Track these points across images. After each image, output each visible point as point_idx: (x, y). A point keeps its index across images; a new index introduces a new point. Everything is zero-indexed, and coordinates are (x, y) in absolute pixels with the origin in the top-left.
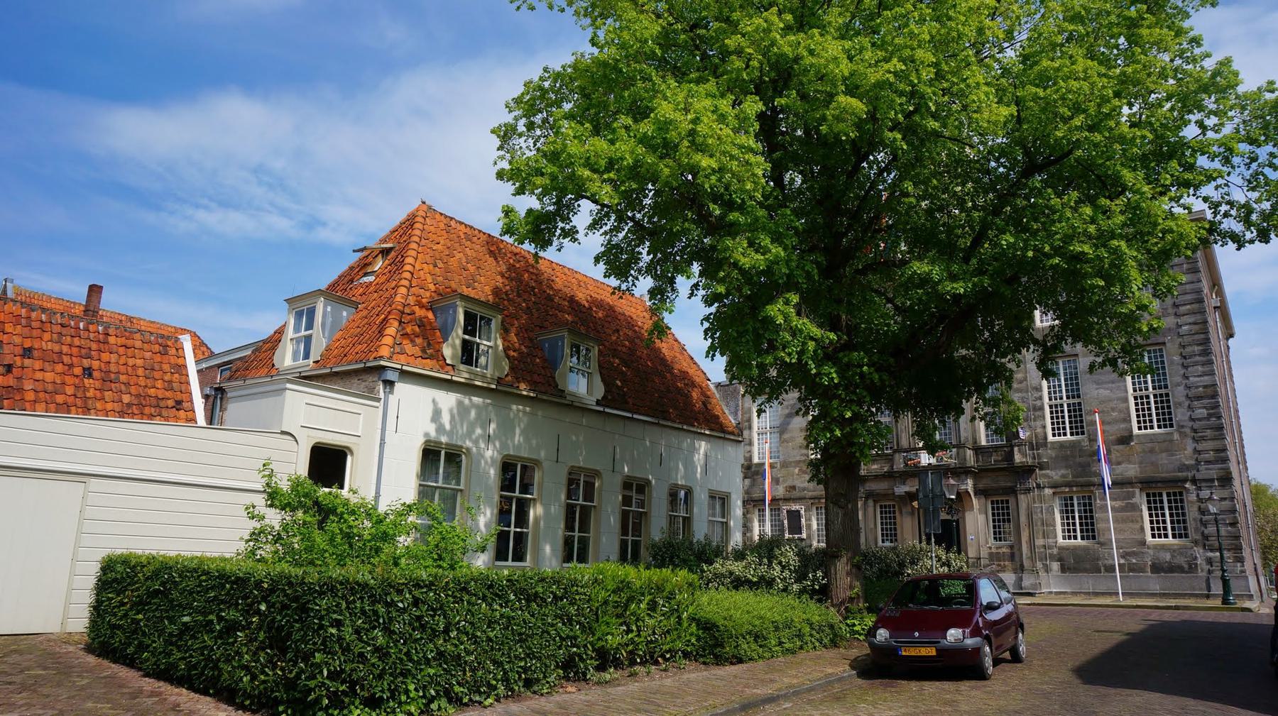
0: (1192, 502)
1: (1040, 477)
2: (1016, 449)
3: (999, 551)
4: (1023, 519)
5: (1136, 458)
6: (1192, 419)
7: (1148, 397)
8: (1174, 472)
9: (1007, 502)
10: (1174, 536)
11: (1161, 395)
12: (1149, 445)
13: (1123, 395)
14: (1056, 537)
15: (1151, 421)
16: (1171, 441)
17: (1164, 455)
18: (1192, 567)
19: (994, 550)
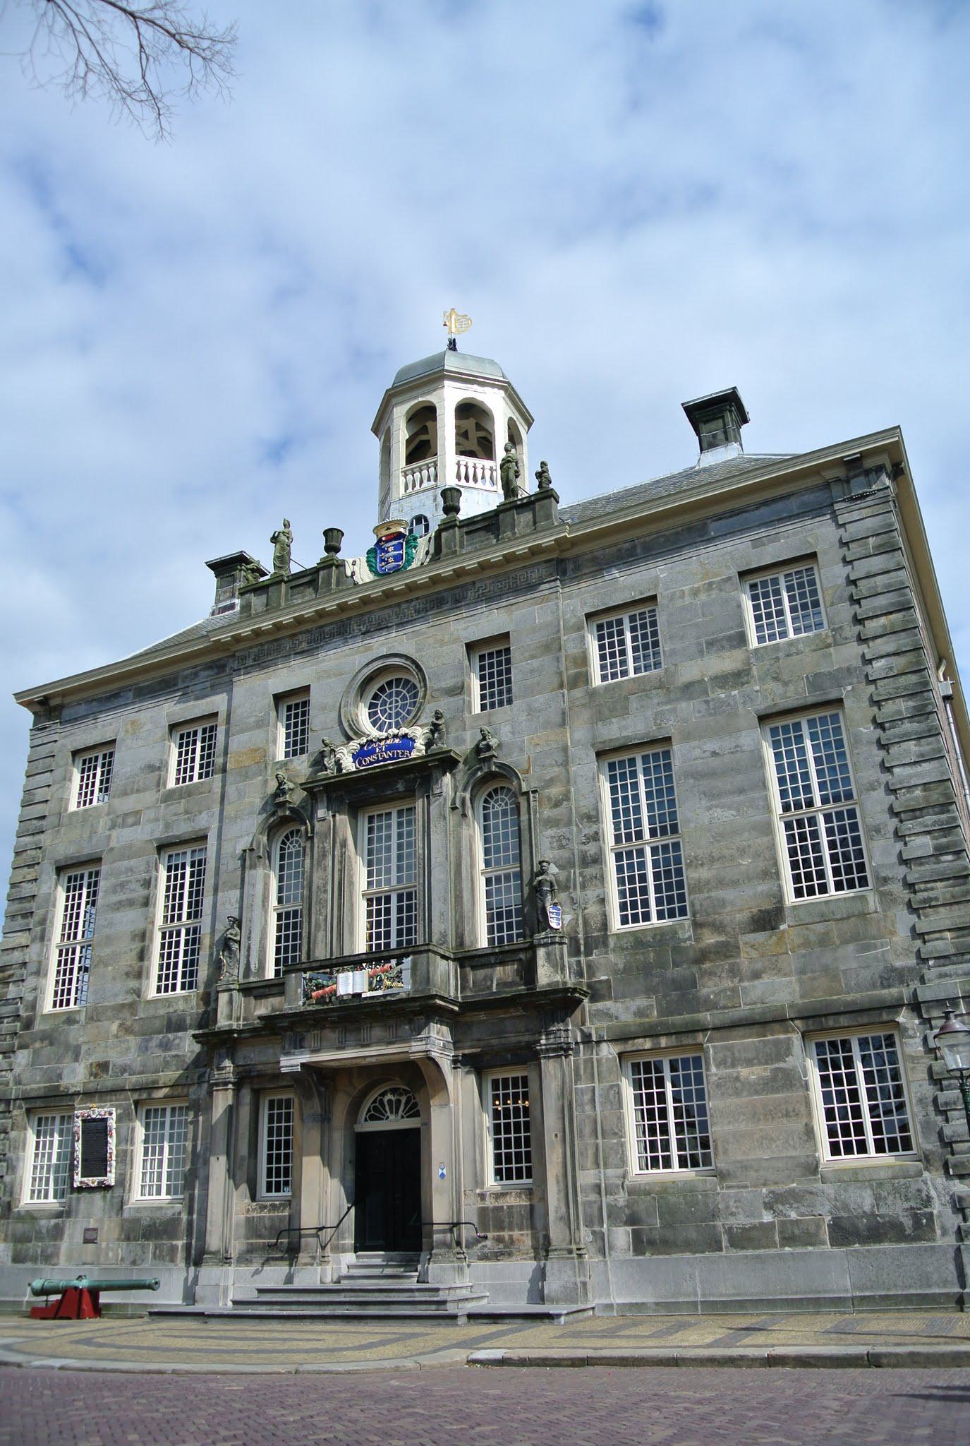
0: (913, 1059)
2: (541, 952)
3: (503, 1203)
4: (551, 1121)
5: (791, 961)
6: (904, 862)
7: (813, 822)
8: (874, 986)
9: (525, 1079)
10: (880, 1148)
11: (840, 816)
12: (820, 928)
13: (759, 817)
14: (623, 1162)
15: (821, 875)
16: (863, 915)
17: (851, 947)
18: (922, 1226)
19: (490, 1203)
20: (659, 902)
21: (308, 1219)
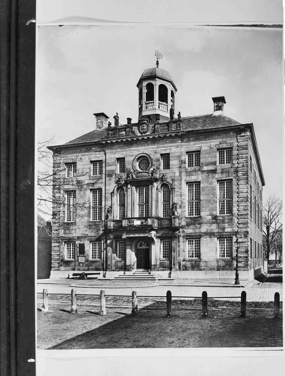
1: (181, 233)
19: (162, 261)
20: (195, 212)
21: (128, 263)
